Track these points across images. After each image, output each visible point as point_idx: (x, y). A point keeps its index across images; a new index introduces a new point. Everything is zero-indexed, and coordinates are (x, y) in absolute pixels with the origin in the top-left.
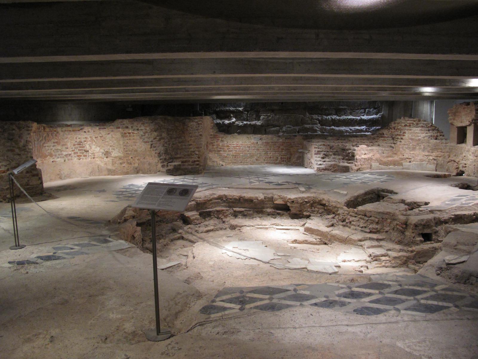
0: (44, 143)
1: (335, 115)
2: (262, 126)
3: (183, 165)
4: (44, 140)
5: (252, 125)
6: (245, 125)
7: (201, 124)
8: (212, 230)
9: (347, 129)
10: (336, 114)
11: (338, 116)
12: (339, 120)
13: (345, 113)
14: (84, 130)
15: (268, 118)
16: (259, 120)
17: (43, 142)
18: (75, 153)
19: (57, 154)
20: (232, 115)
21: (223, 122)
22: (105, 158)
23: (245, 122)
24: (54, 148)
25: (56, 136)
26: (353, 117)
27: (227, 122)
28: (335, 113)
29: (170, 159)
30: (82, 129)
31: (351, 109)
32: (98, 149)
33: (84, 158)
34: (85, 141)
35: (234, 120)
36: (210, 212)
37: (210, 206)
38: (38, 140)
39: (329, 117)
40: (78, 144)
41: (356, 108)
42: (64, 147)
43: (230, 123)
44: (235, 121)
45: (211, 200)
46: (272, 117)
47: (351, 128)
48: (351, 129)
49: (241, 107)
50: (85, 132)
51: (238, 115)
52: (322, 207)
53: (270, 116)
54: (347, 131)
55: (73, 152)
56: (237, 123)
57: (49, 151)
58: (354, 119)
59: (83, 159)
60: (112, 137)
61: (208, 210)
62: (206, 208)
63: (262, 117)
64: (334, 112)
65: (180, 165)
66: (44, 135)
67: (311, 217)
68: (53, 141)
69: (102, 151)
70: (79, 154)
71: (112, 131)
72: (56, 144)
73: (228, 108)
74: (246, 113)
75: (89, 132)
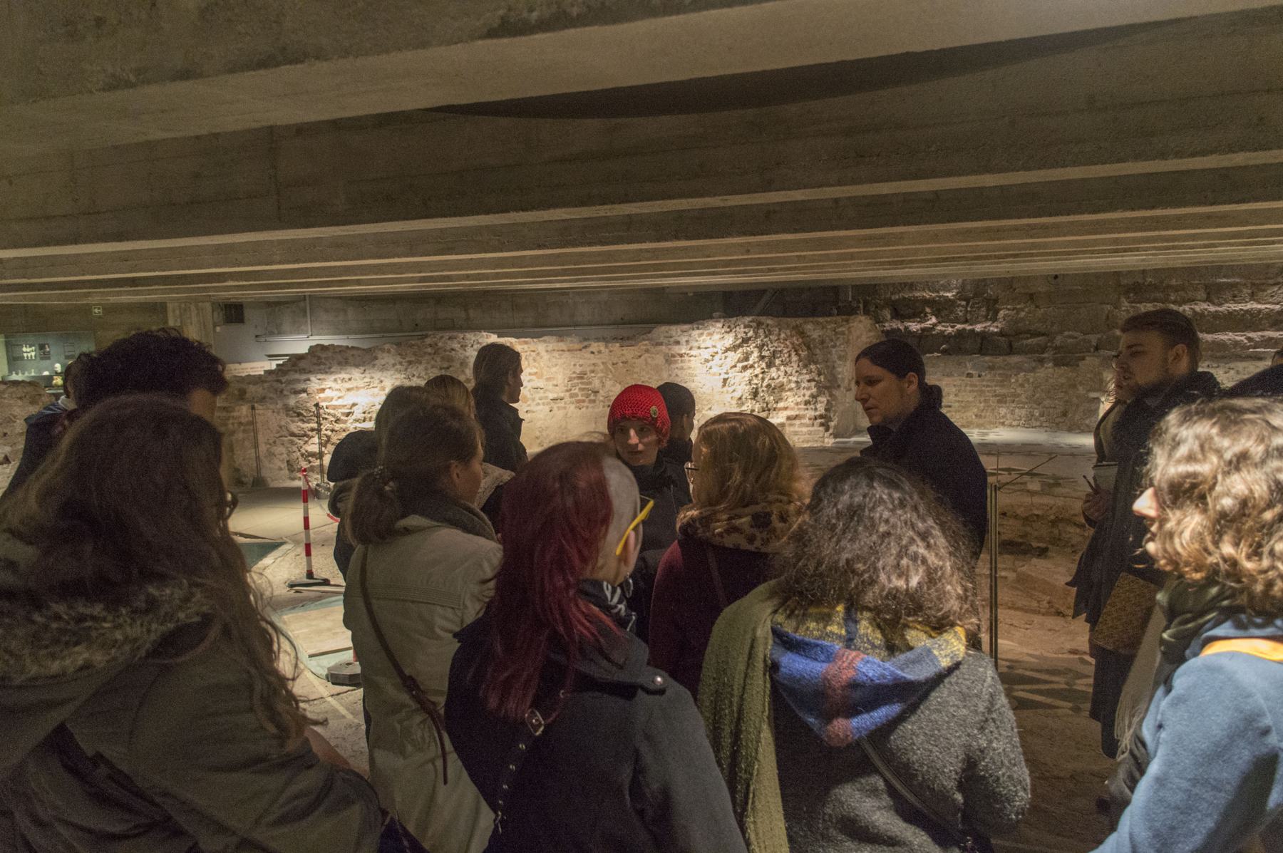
1: (1204, 301)
2: (1001, 334)
3: (791, 425)
5: (978, 334)
6: (960, 334)
7: (843, 333)
9: (1240, 337)
10: (1208, 299)
11: (1214, 304)
12: (1216, 316)
13: (1235, 296)
15: (1018, 313)
16: (994, 319)
19: (537, 396)
20: (928, 310)
21: (906, 328)
23: (959, 326)
26: (1259, 306)
27: (914, 326)
28: (1204, 296)
30: (585, 347)
31: (1253, 284)
35: (934, 320)
39: (1186, 307)
41: (1271, 282)
43: (923, 330)
44: (935, 325)
46: (1029, 312)
47: (1251, 335)
48: (1250, 339)
49: (949, 291)
51: (942, 309)
52: (1078, 530)
53: (1022, 310)
54: (1236, 343)
56: (939, 328)
58: (1260, 311)
60: (647, 363)
63: (1002, 313)
64: (1202, 294)
67: (1049, 554)
71: (647, 351)
72: (533, 377)
73: (918, 294)
74: (964, 303)
75: (600, 352)
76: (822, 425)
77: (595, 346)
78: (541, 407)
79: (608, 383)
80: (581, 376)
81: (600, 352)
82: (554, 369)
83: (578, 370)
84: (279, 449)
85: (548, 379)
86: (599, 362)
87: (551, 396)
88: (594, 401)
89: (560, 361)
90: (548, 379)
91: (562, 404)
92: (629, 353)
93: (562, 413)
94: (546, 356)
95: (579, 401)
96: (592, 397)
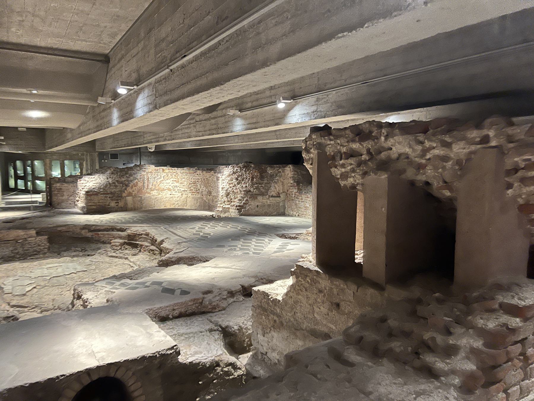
0: (163, 181)
4: (162, 179)
8: (117, 257)
19: (176, 189)
24: (172, 185)
29: (228, 201)
36: (138, 244)
38: (154, 178)
45: (142, 234)
61: (137, 242)
62: (136, 241)
65: (229, 208)
68: (172, 179)
76: (238, 209)
77: (199, 172)
78: (177, 193)
80: (194, 183)
84: (71, 198)
85: (181, 183)
89: (186, 177)
90: (181, 183)
92: (207, 175)
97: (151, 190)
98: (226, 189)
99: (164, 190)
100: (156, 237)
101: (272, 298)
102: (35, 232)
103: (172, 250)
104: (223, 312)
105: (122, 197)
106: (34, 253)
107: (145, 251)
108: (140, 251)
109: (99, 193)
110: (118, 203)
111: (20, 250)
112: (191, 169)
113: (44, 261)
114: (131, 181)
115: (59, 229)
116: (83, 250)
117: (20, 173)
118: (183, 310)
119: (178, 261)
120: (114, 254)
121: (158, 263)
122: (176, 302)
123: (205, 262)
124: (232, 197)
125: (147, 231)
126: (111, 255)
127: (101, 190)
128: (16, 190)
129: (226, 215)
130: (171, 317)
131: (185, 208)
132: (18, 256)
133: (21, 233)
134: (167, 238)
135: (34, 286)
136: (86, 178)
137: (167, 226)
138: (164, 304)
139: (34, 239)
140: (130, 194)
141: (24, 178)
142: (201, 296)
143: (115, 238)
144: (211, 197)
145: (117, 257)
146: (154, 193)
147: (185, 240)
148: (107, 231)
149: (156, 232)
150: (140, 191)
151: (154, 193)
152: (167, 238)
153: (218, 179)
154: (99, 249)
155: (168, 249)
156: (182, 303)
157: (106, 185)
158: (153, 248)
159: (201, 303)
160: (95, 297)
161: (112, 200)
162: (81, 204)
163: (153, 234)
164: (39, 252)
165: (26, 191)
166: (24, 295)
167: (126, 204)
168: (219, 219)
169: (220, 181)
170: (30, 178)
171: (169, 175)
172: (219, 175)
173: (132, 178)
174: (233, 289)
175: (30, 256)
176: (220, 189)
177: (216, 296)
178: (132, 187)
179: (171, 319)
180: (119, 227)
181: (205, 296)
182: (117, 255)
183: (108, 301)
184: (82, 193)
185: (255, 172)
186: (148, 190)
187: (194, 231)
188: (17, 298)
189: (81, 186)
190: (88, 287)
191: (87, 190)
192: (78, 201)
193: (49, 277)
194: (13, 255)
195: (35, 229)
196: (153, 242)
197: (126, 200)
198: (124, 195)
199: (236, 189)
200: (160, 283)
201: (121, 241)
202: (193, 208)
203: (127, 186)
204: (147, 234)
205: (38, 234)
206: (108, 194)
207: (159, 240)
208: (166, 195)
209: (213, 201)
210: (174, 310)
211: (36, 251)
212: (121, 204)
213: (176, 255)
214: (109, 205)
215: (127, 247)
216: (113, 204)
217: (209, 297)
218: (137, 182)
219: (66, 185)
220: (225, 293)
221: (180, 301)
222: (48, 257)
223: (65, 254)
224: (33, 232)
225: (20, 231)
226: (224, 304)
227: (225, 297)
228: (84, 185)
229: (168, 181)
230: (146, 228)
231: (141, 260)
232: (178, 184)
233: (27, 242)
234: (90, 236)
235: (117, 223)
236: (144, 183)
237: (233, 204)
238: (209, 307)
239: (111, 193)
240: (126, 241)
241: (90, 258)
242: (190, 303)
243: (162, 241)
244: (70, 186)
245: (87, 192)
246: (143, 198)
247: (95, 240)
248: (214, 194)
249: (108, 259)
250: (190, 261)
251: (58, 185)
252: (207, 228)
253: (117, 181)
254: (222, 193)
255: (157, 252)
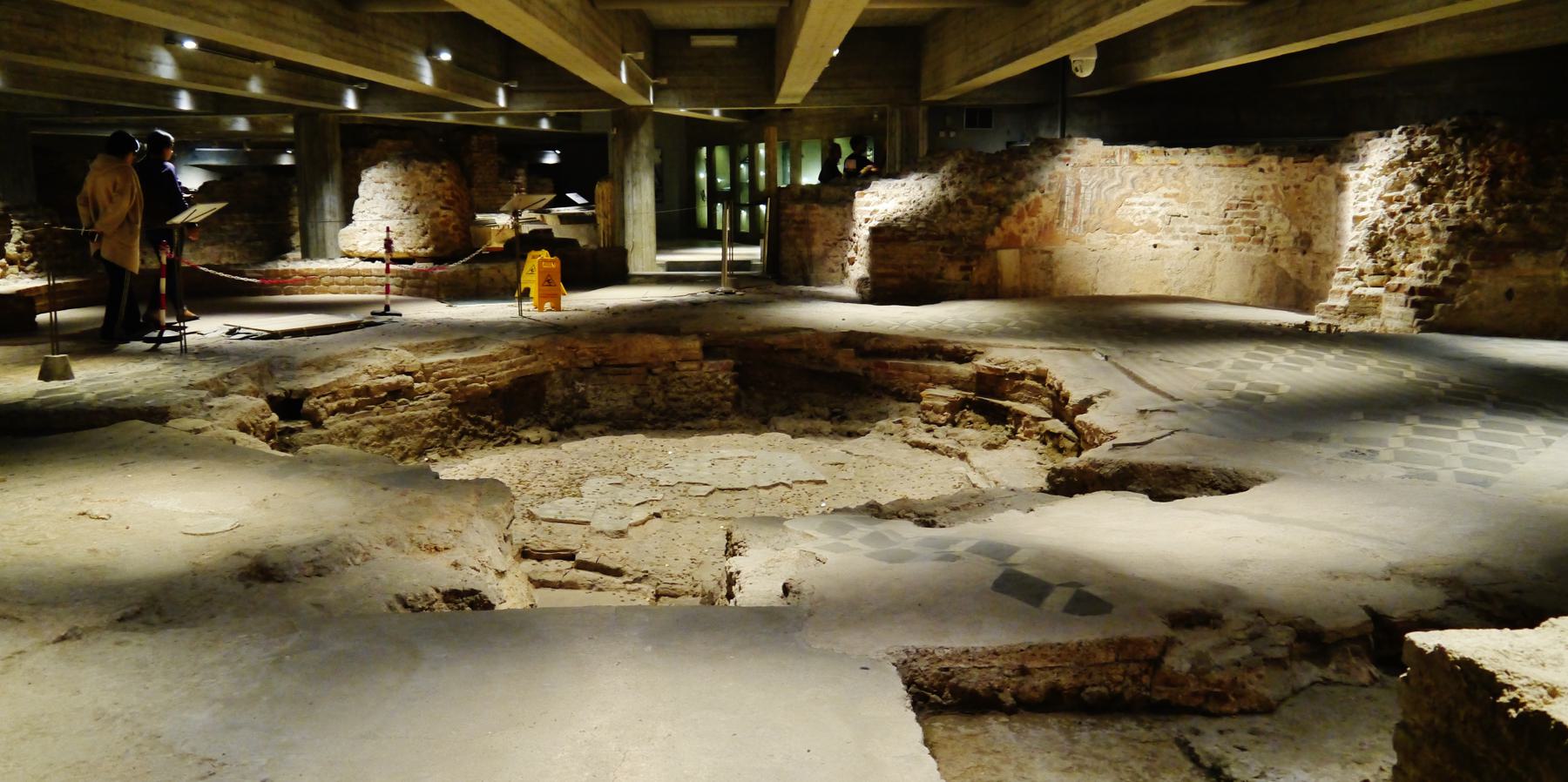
0: (1129, 195)
4: (1128, 188)
8: (934, 448)
14: (1260, 165)
17: (1123, 191)
18: (1229, 232)
22: (1299, 255)
25: (1175, 177)
29: (1377, 272)
30: (1253, 162)
32: (1285, 225)
33: (1255, 246)
34: (1260, 198)
36: (1007, 409)
37: (1016, 395)
38: (1100, 186)
40: (1245, 206)
42: (1199, 211)
45: (1023, 375)
50: (1261, 170)
55: (1225, 227)
57: (1145, 217)
59: (1249, 249)
61: (1007, 403)
65: (1377, 300)
66: (1132, 175)
68: (1164, 190)
69: (1294, 230)
70: (1242, 234)
71: (1321, 170)
72: (1173, 200)
75: (1271, 170)
77: (1267, 161)
79: (1277, 216)
80: (1247, 203)
81: (1271, 170)
82: (1206, 192)
83: (1242, 194)
86: (1269, 184)
87: (1199, 228)
88: (1262, 241)
89: (1216, 181)
91: (1213, 240)
92: (1300, 171)
93: (1211, 253)
94: (1195, 172)
95: (1239, 240)
96: (1260, 236)
97: (1086, 230)
98: (1370, 221)
99: (1131, 229)
100: (1067, 388)
101: (1515, 703)
102: (697, 344)
103: (1111, 436)
104: (1261, 722)
105: (982, 248)
106: (696, 411)
107: (1029, 435)
108: (1014, 432)
109: (912, 234)
110: (970, 268)
111: (658, 400)
112: (1240, 150)
113: (711, 439)
114: (1020, 195)
115: (769, 340)
116: (835, 414)
117: (723, 181)
118: (1065, 681)
119: (1123, 479)
120: (927, 439)
121: (1049, 479)
122: (1036, 640)
123: (1228, 492)
124: (1397, 255)
125: (1043, 366)
126: (915, 438)
127: (920, 225)
128: (710, 236)
129: (1365, 325)
130: (1007, 698)
131: (1206, 296)
132: (651, 416)
133: (660, 344)
134: (1107, 393)
135: (658, 510)
136: (880, 187)
137: (1116, 352)
138: (980, 641)
139: (694, 366)
140: (1012, 242)
141: (731, 199)
142: (1161, 630)
143: (937, 382)
144: (1309, 257)
145: (934, 448)
146: (1097, 239)
147: (1168, 404)
148: (914, 358)
149: (1073, 369)
150: (1046, 230)
151: (1097, 239)
152: (1107, 393)
153: (1341, 185)
154: (884, 415)
155: (1097, 431)
156: (1062, 646)
157: (938, 208)
158: (1057, 426)
159: (1155, 663)
160: (760, 577)
161: (951, 259)
162: (859, 270)
163: (1060, 378)
164: (708, 409)
165: (740, 239)
166: (621, 534)
167: (996, 274)
168: (1331, 338)
169: (1350, 193)
170: (745, 198)
171: (1155, 174)
172: (1349, 170)
173: (1022, 185)
174: (1327, 624)
175: (684, 420)
176: (1349, 224)
177: (1231, 643)
178: (1020, 217)
179: (1010, 711)
180: (950, 347)
181: (1181, 635)
182: (934, 442)
183: (786, 589)
184: (862, 234)
185: (1510, 150)
186: (1076, 230)
187: (1214, 375)
188: (601, 538)
189: (863, 212)
190: (765, 532)
191: (874, 223)
192: (852, 261)
193: (709, 489)
194: (636, 410)
195: (701, 335)
196: (1059, 404)
197: (996, 262)
198: (991, 242)
199: (1417, 221)
200: (997, 552)
201: (953, 393)
202: (1237, 297)
203: (1004, 211)
204: (1040, 377)
205: (710, 351)
206: (939, 238)
207: (1076, 397)
208: (1139, 244)
209: (1315, 272)
210: (1024, 671)
211: (698, 404)
212: (979, 274)
213: (1118, 456)
214: (940, 276)
215: (971, 415)
216: (953, 273)
217: (1200, 642)
218: (1037, 201)
219: (821, 210)
220: (1283, 636)
221: (1058, 637)
222: (730, 429)
223: (783, 423)
224: (693, 345)
225: (658, 339)
226: (1266, 686)
227: (1278, 653)
228: (871, 209)
229: (1145, 198)
230: (1037, 354)
231: (1018, 463)
232: (1183, 210)
233: (677, 375)
234: (860, 372)
235: (950, 332)
236: (1062, 203)
237: (1396, 281)
238: (1193, 686)
239: (951, 235)
240: (971, 394)
241: (848, 444)
242: (1102, 657)
243: (1087, 403)
244: (833, 214)
245: (874, 230)
246: (1056, 257)
247: (875, 387)
248: (1321, 244)
249: (905, 452)
250: (1166, 484)
251: (799, 208)
252: (1266, 366)
253: (973, 196)
254: (1354, 236)
255: (1070, 444)
